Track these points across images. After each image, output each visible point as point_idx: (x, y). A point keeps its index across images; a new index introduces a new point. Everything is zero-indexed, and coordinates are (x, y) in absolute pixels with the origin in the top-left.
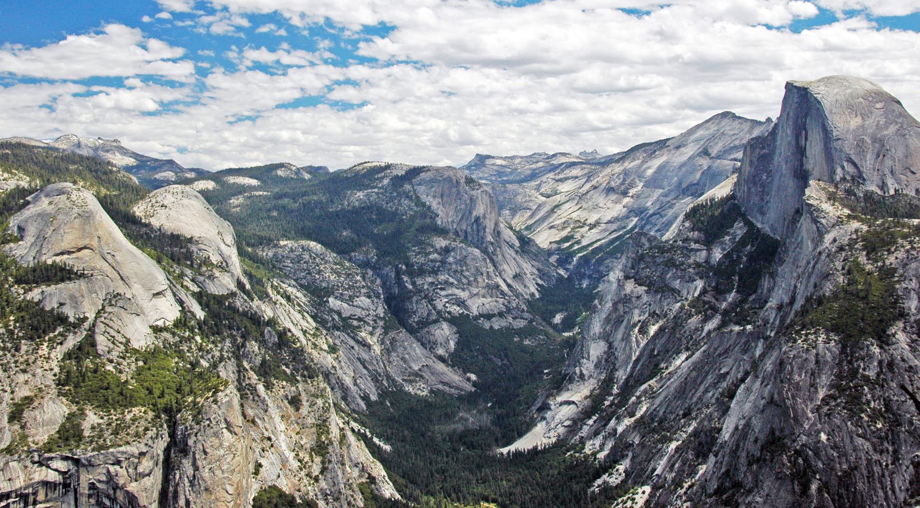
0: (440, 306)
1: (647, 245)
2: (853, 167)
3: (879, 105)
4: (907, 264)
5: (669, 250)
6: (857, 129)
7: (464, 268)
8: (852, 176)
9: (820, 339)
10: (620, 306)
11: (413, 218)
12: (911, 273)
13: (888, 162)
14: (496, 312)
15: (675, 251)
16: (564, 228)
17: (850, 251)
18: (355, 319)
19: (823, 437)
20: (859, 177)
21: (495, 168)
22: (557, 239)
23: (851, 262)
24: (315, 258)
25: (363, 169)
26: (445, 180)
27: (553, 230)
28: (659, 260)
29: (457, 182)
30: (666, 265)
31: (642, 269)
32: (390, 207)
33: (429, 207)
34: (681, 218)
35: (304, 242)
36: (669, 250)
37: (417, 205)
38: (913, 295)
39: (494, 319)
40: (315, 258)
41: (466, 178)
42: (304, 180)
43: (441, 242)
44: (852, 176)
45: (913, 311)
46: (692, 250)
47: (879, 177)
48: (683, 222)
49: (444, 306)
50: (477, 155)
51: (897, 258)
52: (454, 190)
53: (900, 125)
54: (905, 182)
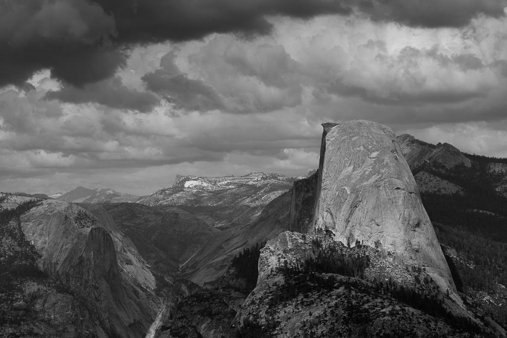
1: (187, 293)
2: (330, 217)
3: (374, 154)
4: (290, 318)
5: (207, 299)
6: (344, 179)
7: (52, 317)
8: (326, 227)
11: (12, 259)
12: (290, 326)
13: (358, 213)
15: (214, 300)
16: (222, 267)
17: (259, 305)
20: (334, 228)
22: (213, 280)
23: (254, 315)
26: (54, 215)
27: (211, 269)
28: (196, 309)
29: (66, 217)
30: (202, 315)
31: (179, 319)
33: (33, 246)
36: (207, 299)
37: (19, 245)
41: (79, 214)
43: (32, 287)
44: (326, 227)
46: (231, 298)
48: (229, 268)
50: (178, 177)
51: (285, 312)
53: (380, 176)
54: (369, 234)
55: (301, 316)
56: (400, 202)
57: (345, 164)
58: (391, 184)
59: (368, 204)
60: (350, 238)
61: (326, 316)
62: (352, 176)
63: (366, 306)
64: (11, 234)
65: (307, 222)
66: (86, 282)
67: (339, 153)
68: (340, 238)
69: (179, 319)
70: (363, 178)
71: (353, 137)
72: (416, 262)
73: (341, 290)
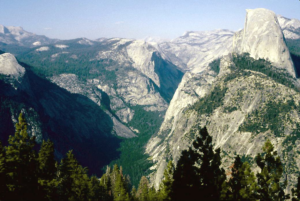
0: (126, 100)
1: (191, 77)
2: (249, 47)
4: (232, 86)
6: (255, 32)
9: (192, 114)
10: (178, 101)
12: (232, 90)
13: (260, 46)
14: (153, 104)
15: (201, 79)
16: (204, 66)
18: (87, 106)
19: (178, 147)
21: (193, 37)
22: (200, 72)
24: (74, 81)
25: (111, 41)
26: (139, 47)
28: (195, 83)
29: (143, 47)
30: (197, 85)
31: (188, 87)
32: (114, 59)
34: (208, 65)
35: (70, 74)
36: (198, 79)
38: (229, 98)
39: (151, 107)
40: (74, 81)
42: (90, 46)
45: (226, 103)
47: (256, 52)
49: (129, 101)
52: (142, 51)
55: (237, 86)
56: (277, 42)
57: (255, 26)
58: (273, 34)
59: (263, 43)
60: (257, 56)
61: (246, 86)
62: (258, 31)
63: (263, 83)
64: (123, 54)
65: (239, 49)
66: (152, 72)
67: (253, 22)
68: (252, 55)
69: (188, 87)
70: (262, 32)
71: (258, 15)
72: (283, 66)
73: (253, 76)
